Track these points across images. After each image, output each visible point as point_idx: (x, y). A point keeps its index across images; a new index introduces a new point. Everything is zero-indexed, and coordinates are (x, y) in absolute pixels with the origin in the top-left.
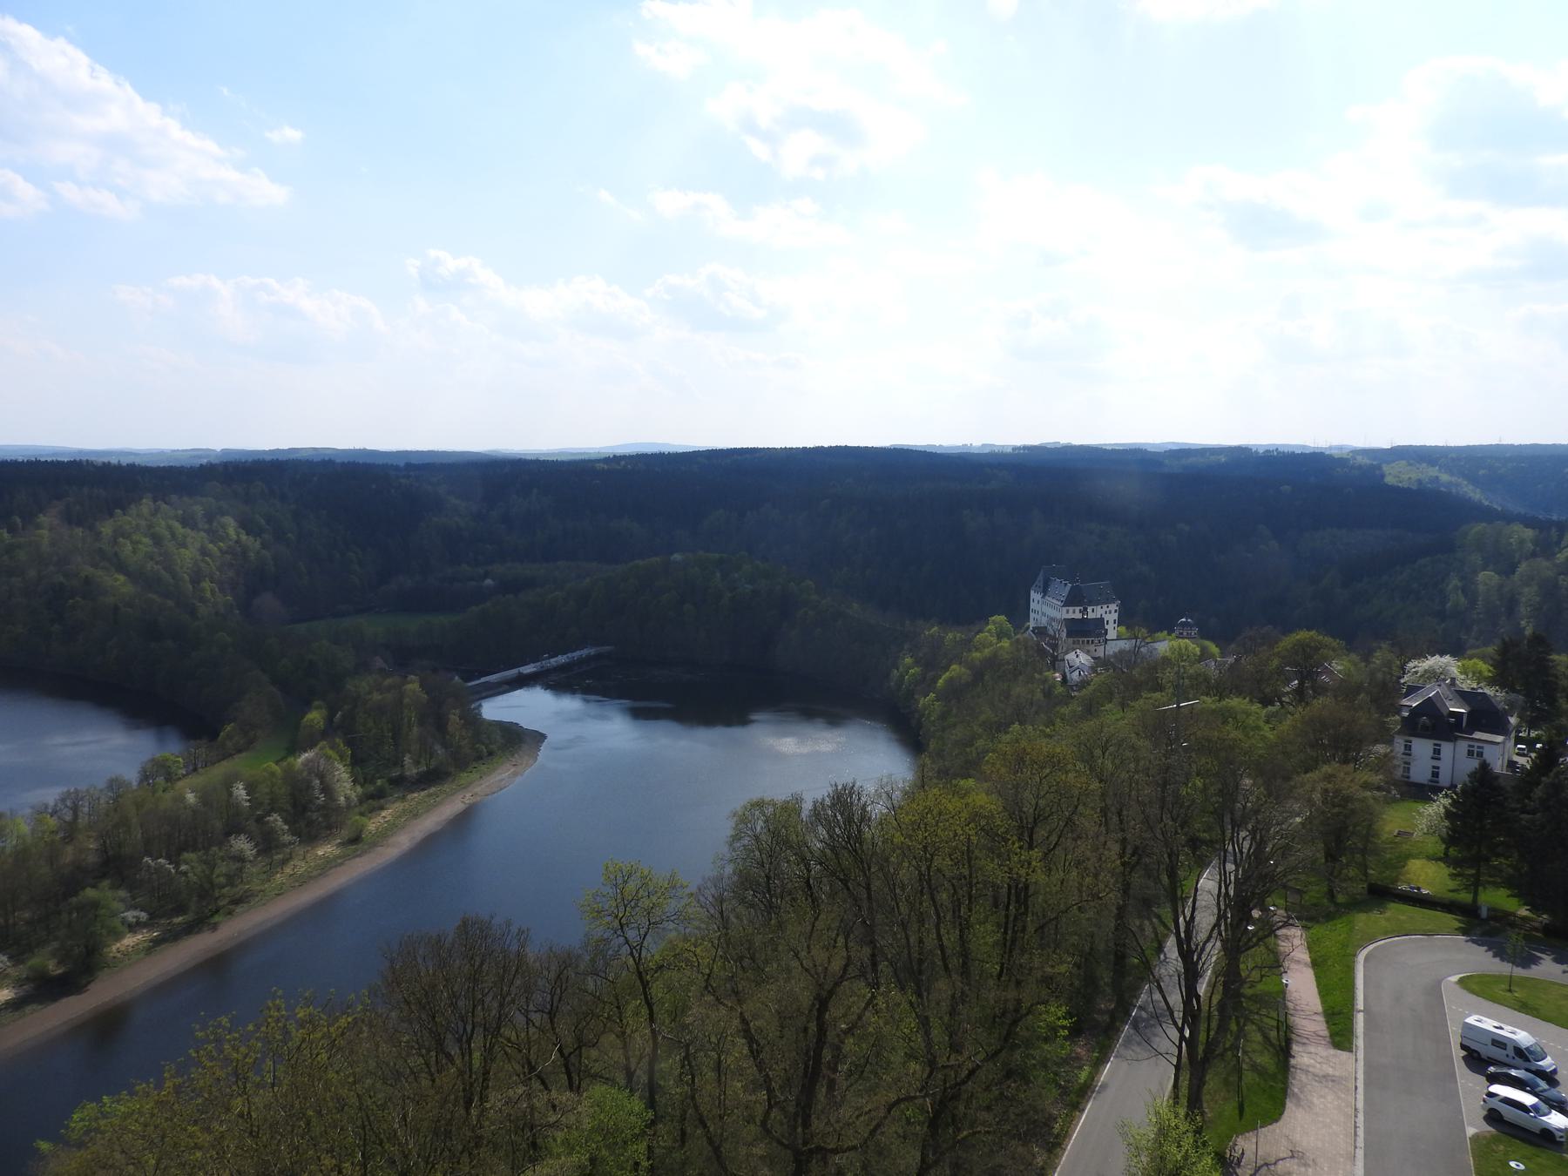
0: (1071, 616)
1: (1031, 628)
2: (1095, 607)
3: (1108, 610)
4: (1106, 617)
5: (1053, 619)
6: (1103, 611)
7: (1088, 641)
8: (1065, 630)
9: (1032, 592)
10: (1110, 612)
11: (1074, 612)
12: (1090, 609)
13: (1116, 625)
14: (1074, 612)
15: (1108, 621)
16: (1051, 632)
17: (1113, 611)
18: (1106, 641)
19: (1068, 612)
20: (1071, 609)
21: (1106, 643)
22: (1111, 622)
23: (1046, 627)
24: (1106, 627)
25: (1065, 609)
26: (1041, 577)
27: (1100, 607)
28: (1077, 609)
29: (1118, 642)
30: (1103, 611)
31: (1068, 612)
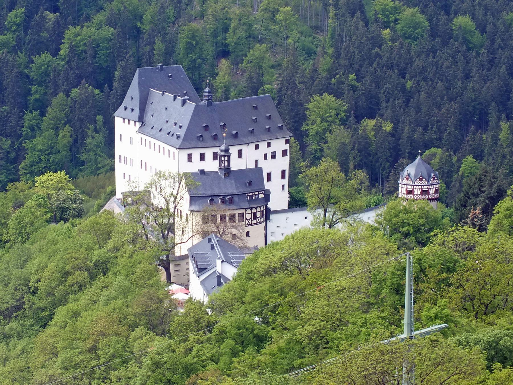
0: (196, 166)
2: (243, 148)
4: (266, 166)
5: (161, 175)
6: (258, 155)
7: (233, 217)
8: (187, 196)
9: (118, 121)
10: (273, 156)
11: (202, 157)
12: (234, 151)
13: (286, 182)
14: (202, 157)
15: (269, 175)
16: (158, 201)
17: (279, 154)
18: (268, 214)
19: (190, 157)
20: (196, 154)
21: (267, 219)
22: (276, 176)
24: (267, 186)
25: (184, 153)
26: (134, 90)
27: (252, 146)
28: (209, 153)
30: (258, 155)
31: (190, 157)
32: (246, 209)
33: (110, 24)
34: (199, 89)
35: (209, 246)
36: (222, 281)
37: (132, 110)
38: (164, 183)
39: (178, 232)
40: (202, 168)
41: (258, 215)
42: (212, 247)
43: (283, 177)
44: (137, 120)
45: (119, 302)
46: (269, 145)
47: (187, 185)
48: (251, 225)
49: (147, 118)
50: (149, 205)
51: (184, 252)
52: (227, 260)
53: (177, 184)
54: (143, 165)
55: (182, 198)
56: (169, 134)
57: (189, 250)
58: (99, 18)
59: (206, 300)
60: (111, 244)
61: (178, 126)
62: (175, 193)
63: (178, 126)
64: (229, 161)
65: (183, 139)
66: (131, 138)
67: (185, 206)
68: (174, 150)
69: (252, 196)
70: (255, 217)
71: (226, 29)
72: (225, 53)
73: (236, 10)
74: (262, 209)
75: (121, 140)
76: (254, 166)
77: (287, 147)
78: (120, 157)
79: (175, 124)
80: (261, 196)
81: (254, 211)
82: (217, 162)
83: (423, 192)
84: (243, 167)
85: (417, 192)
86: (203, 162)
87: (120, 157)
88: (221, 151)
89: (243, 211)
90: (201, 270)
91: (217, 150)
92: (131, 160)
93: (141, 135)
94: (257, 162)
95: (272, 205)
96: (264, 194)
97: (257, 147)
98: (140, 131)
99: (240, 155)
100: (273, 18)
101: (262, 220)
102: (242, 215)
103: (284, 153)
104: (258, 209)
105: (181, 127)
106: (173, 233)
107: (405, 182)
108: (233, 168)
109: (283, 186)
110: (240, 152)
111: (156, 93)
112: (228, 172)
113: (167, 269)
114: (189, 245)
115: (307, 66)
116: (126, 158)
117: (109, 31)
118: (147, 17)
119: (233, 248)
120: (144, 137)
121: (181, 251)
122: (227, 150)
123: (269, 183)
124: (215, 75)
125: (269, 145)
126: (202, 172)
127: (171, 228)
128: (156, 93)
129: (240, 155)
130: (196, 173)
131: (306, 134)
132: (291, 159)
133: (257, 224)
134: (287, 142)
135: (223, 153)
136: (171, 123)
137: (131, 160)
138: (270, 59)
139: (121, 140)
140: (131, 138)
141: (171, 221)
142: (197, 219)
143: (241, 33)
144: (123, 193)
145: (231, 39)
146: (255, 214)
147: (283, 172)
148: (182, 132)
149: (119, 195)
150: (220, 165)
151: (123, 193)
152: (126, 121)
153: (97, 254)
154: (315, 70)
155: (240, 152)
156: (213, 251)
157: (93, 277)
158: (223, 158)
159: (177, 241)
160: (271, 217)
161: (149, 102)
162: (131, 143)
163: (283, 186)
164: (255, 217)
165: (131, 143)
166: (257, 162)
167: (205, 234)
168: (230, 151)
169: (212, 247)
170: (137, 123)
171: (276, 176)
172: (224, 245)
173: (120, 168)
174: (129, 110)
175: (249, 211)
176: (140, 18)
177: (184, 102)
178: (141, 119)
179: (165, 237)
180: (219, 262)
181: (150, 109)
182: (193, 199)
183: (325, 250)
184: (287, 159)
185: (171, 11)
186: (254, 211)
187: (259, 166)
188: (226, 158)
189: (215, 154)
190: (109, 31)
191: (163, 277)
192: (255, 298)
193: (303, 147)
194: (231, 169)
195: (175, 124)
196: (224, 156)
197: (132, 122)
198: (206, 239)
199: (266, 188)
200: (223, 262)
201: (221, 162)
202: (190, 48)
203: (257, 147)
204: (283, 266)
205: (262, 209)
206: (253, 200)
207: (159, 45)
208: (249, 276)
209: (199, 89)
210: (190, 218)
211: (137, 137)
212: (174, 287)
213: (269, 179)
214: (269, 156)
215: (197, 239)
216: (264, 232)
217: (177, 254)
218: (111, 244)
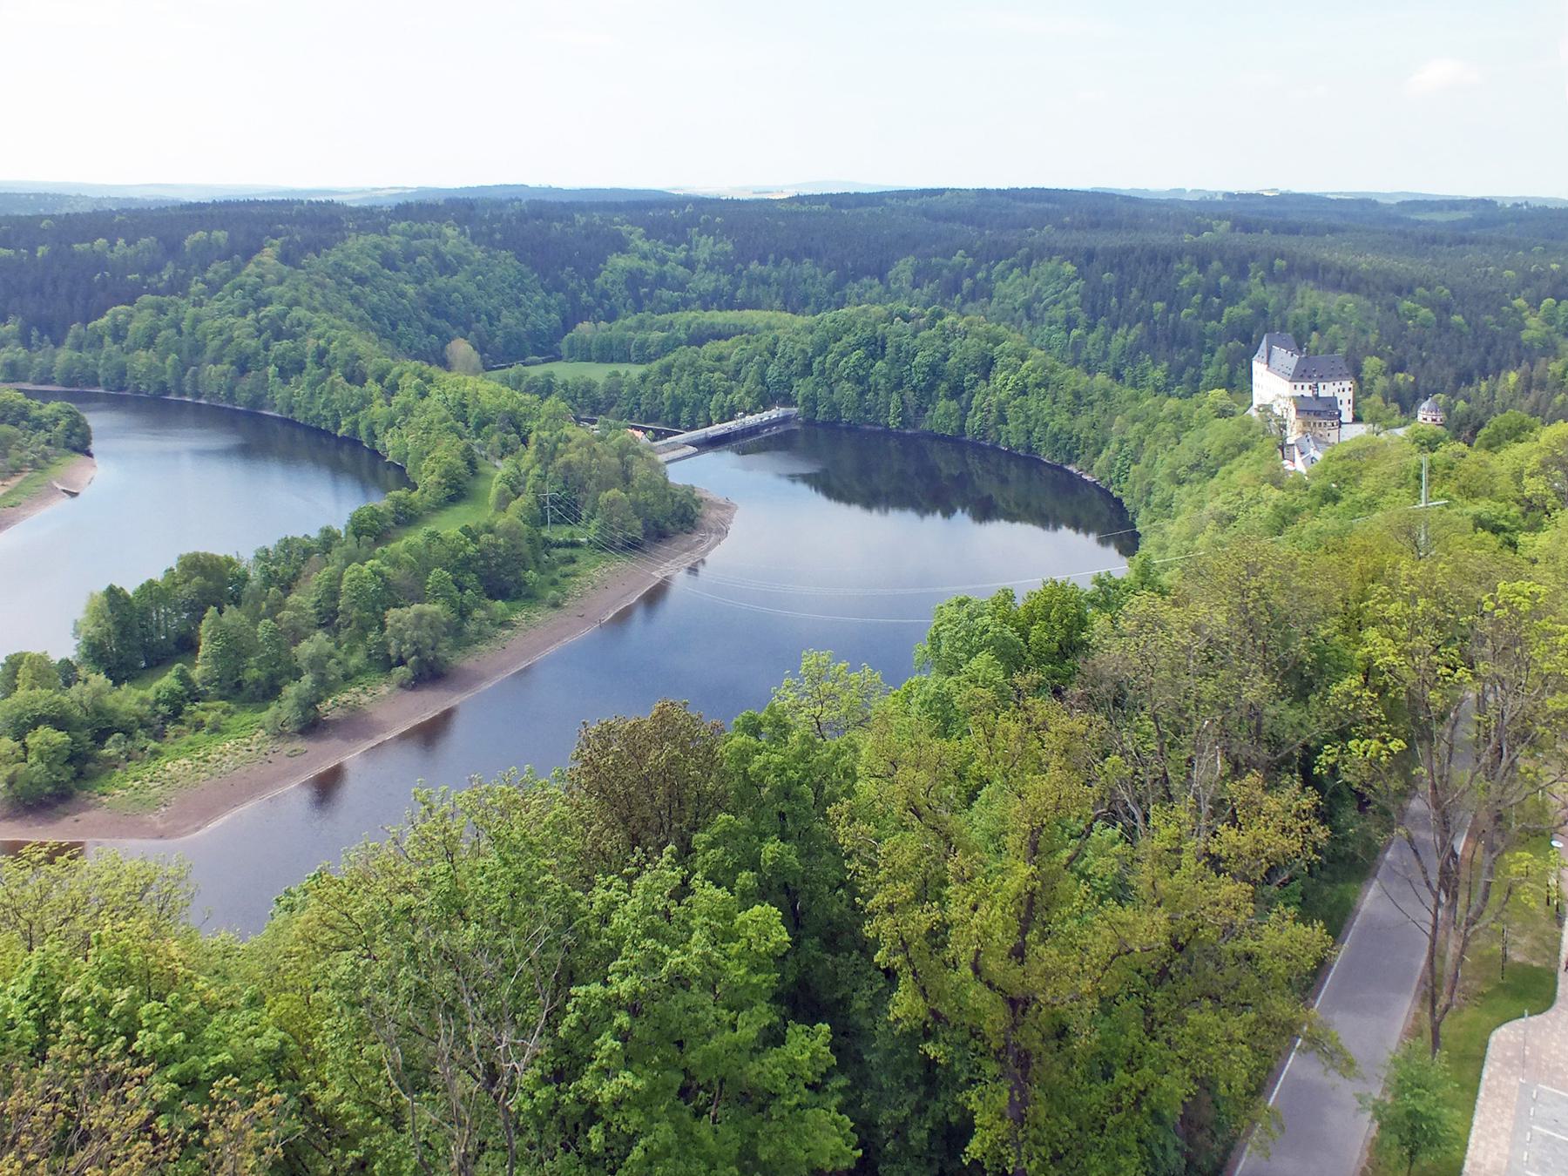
0: (1299, 393)
3: (1341, 387)
4: (1340, 396)
5: (1279, 396)
8: (1294, 410)
16: (1277, 411)
18: (1341, 423)
20: (1299, 385)
22: (1345, 402)
24: (1340, 407)
26: (1264, 345)
28: (1307, 385)
33: (1251, 307)
34: (1300, 348)
38: (1280, 401)
45: (1255, 467)
52: (1317, 449)
58: (1243, 303)
59: (1304, 471)
60: (1250, 433)
67: (1293, 414)
71: (1315, 314)
72: (1315, 328)
73: (1321, 304)
85: (1429, 419)
90: (1302, 453)
100: (1342, 310)
112: (1317, 397)
115: (1364, 339)
117: (1249, 311)
118: (1270, 305)
119: (1320, 442)
121: (1290, 441)
124: (1309, 341)
127: (1285, 427)
131: (1362, 379)
138: (1341, 334)
142: (1299, 423)
143: (1325, 317)
145: (1319, 320)
148: (1291, 372)
149: (1255, 406)
153: (1243, 438)
154: (1367, 342)
157: (1240, 452)
167: (1304, 433)
171: (1345, 402)
172: (1316, 441)
176: (1267, 305)
178: (1268, 363)
181: (1273, 357)
182: (1298, 411)
183: (1375, 448)
185: (1285, 302)
190: (1249, 311)
191: (1280, 455)
192: (1333, 473)
193: (1361, 387)
202: (1296, 324)
204: (1349, 456)
206: (1332, 417)
207: (1277, 321)
208: (1330, 459)
209: (1300, 348)
212: (1285, 462)
215: (1300, 435)
218: (1250, 433)
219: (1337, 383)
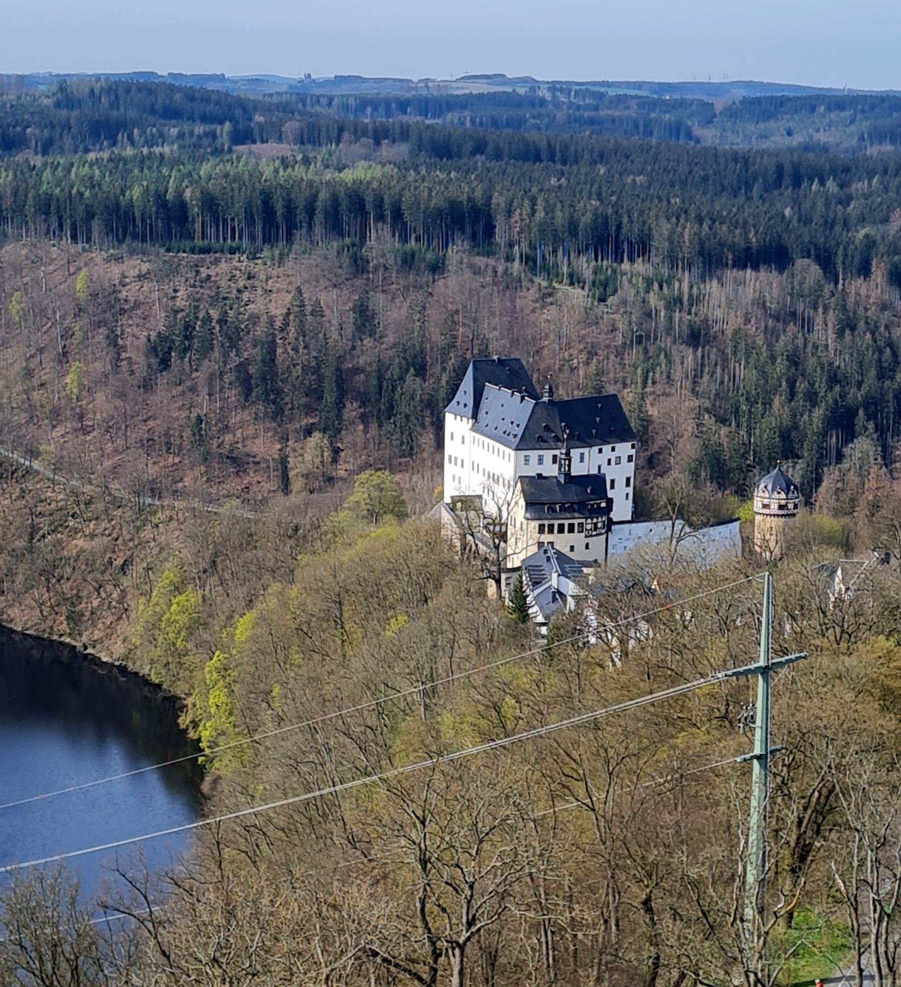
1: (447, 499)
2: (586, 451)
4: (609, 473)
6: (602, 459)
7: (571, 527)
8: (522, 502)
9: (449, 418)
10: (618, 462)
11: (541, 460)
12: (575, 453)
13: (630, 490)
14: (541, 460)
15: (613, 481)
16: (490, 508)
17: (624, 459)
18: (610, 523)
19: (527, 459)
20: (534, 455)
21: (609, 530)
22: (620, 483)
23: (480, 497)
24: (610, 493)
26: (468, 384)
27: (595, 449)
28: (548, 455)
29: (633, 525)
30: (602, 459)
31: (527, 459)
32: (587, 518)
35: (544, 557)
36: (557, 596)
37: (465, 405)
39: (511, 541)
40: (539, 472)
41: (599, 525)
42: (548, 559)
43: (628, 485)
44: (470, 416)
46: (613, 449)
47: (523, 491)
48: (591, 536)
49: (481, 414)
50: (479, 510)
51: (517, 564)
53: (512, 489)
54: (475, 467)
55: (516, 503)
56: (504, 433)
57: (523, 561)
61: (515, 425)
62: (509, 498)
63: (515, 425)
64: (569, 466)
65: (521, 440)
66: (463, 437)
67: (520, 511)
68: (510, 451)
69: (592, 505)
70: (596, 528)
74: (604, 519)
75: (452, 439)
76: (596, 472)
77: (633, 452)
78: (450, 457)
79: (512, 423)
80: (603, 505)
81: (595, 520)
82: (556, 466)
83: (781, 507)
84: (586, 473)
86: (541, 466)
87: (450, 457)
88: (561, 454)
89: (583, 521)
91: (557, 452)
92: (462, 461)
93: (474, 434)
94: (599, 467)
95: (615, 516)
96: (606, 502)
97: (600, 451)
98: (473, 429)
99: (582, 461)
101: (603, 531)
102: (581, 525)
103: (630, 459)
104: (600, 519)
105: (518, 426)
106: (505, 542)
107: (761, 494)
108: (574, 473)
109: (627, 495)
110: (582, 455)
111: (491, 389)
112: (568, 475)
113: (498, 582)
114: (522, 556)
116: (456, 458)
120: (477, 436)
122: (568, 454)
123: (613, 491)
125: (613, 449)
126: (540, 476)
127: (503, 537)
128: (491, 389)
129: (582, 461)
130: (534, 477)
132: (636, 465)
133: (597, 535)
134: (633, 446)
135: (563, 456)
136: (508, 420)
137: (462, 461)
139: (452, 439)
140: (463, 437)
141: (504, 529)
144: (452, 497)
146: (596, 524)
147: (628, 479)
149: (447, 499)
150: (560, 469)
151: (452, 497)
152: (459, 418)
155: (582, 455)
156: (549, 564)
158: (563, 462)
159: (510, 551)
160: (614, 527)
161: (484, 397)
162: (463, 442)
163: (627, 495)
164: (596, 528)
165: (463, 442)
166: (599, 467)
168: (572, 455)
169: (548, 559)
170: (470, 421)
171: (620, 483)
173: (449, 469)
174: (462, 405)
175: (589, 521)
177: (522, 399)
178: (475, 416)
179: (497, 547)
180: (555, 576)
181: (484, 405)
182: (529, 505)
184: (633, 464)
186: (595, 520)
187: (602, 472)
188: (567, 462)
189: (555, 457)
194: (573, 474)
195: (512, 423)
196: (565, 460)
197: (465, 419)
198: (542, 551)
199: (609, 496)
200: (559, 575)
201: (560, 466)
203: (600, 451)
205: (604, 519)
210: (524, 527)
211: (470, 435)
213: (612, 487)
214: (613, 462)
216: (604, 544)
217: (509, 566)
219: (607, 448)
